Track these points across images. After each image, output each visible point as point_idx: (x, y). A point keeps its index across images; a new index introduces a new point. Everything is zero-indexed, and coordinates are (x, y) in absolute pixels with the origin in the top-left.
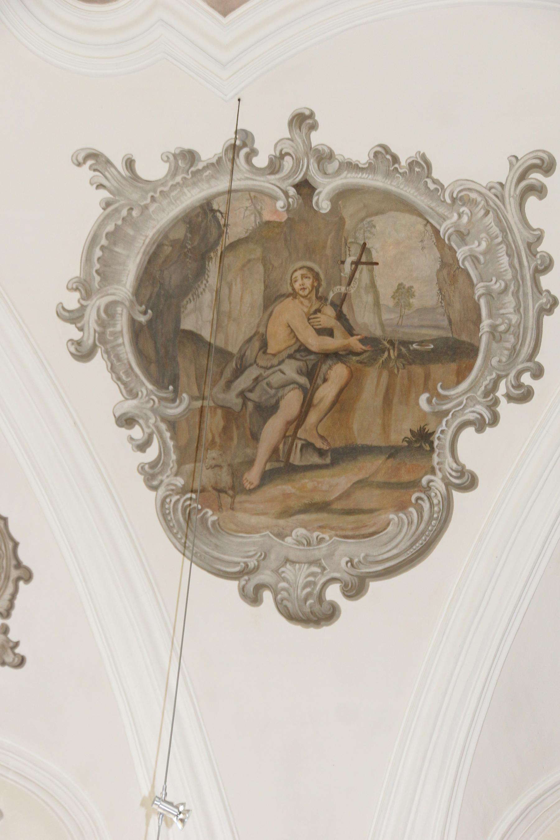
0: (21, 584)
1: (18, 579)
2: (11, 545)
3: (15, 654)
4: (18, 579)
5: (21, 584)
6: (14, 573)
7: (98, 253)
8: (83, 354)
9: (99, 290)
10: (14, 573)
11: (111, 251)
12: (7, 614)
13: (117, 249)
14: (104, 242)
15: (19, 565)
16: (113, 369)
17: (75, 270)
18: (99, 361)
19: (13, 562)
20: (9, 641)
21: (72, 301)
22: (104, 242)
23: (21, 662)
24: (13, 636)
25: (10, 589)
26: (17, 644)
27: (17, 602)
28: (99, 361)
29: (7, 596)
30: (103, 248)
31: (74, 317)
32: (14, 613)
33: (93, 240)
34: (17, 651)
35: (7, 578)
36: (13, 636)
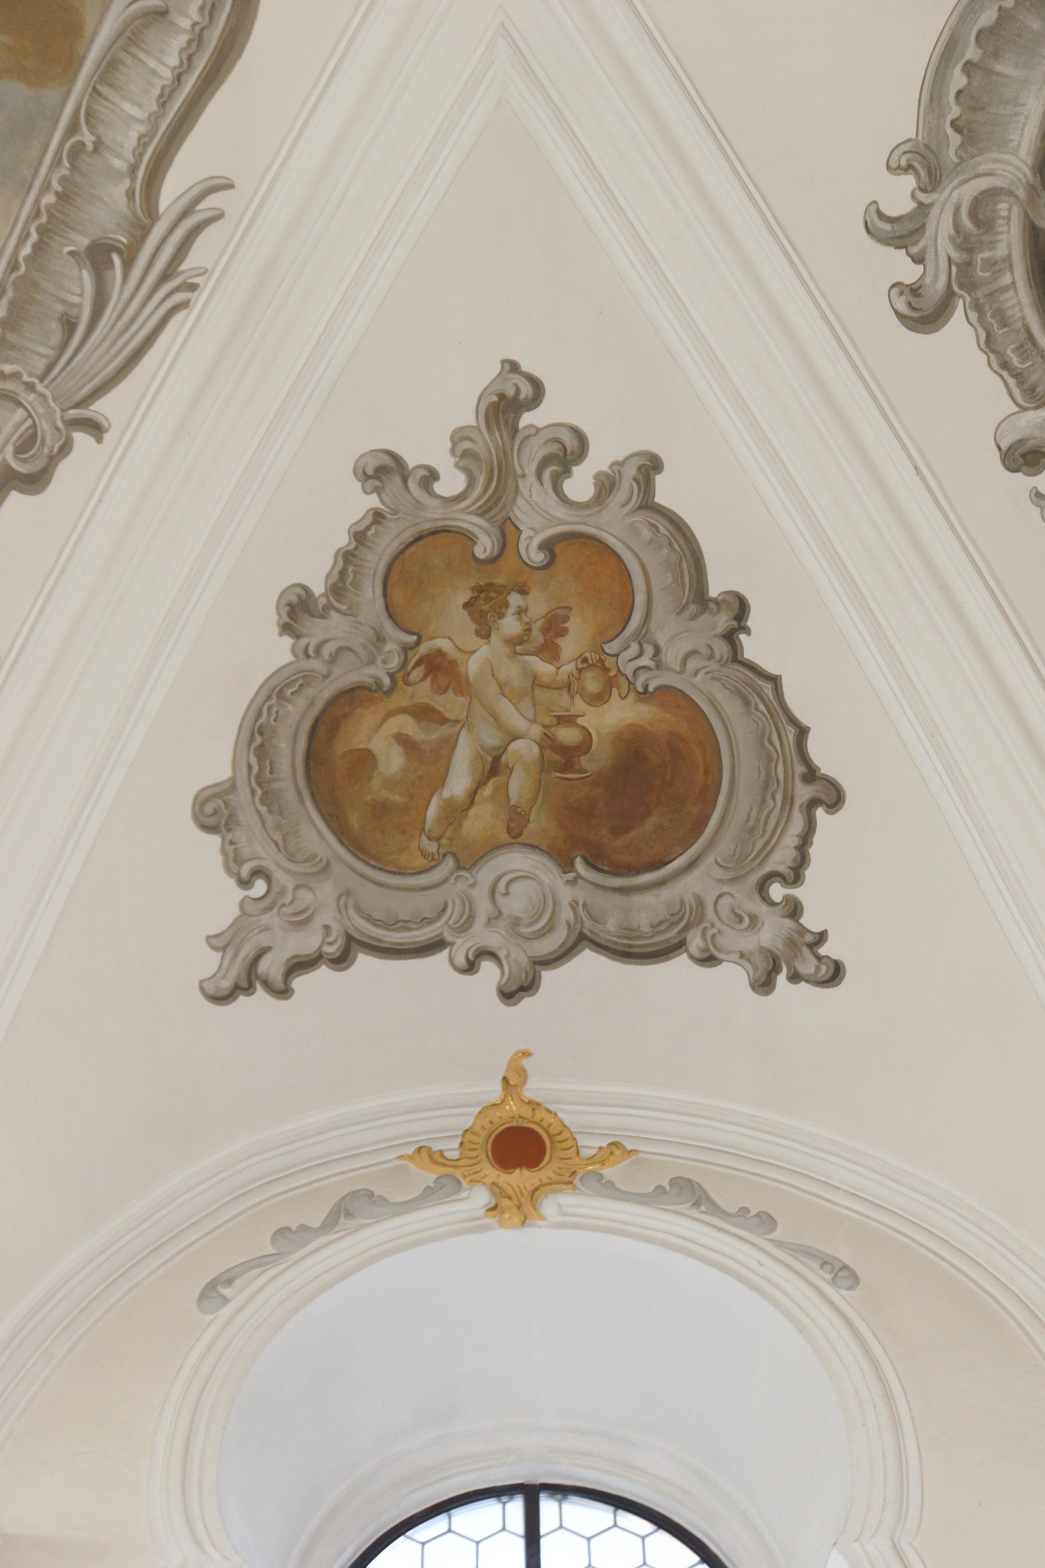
0: (820, 813)
1: (813, 804)
2: (791, 733)
3: (819, 958)
4: (813, 804)
5: (820, 813)
6: (803, 793)
7: (958, 80)
8: (924, 314)
9: (959, 164)
10: (803, 793)
11: (989, 72)
12: (796, 875)
13: (1000, 68)
14: (972, 53)
15: (811, 775)
16: (990, 345)
17: (905, 125)
18: (959, 330)
19: (800, 769)
20: (803, 930)
21: (899, 196)
22: (972, 53)
23: (835, 974)
24: (811, 921)
25: (797, 825)
26: (821, 937)
27: (813, 851)
28: (959, 330)
29: (791, 838)
30: (969, 68)
31: (900, 233)
33: (948, 52)
34: (823, 951)
35: (789, 801)
36: (811, 921)
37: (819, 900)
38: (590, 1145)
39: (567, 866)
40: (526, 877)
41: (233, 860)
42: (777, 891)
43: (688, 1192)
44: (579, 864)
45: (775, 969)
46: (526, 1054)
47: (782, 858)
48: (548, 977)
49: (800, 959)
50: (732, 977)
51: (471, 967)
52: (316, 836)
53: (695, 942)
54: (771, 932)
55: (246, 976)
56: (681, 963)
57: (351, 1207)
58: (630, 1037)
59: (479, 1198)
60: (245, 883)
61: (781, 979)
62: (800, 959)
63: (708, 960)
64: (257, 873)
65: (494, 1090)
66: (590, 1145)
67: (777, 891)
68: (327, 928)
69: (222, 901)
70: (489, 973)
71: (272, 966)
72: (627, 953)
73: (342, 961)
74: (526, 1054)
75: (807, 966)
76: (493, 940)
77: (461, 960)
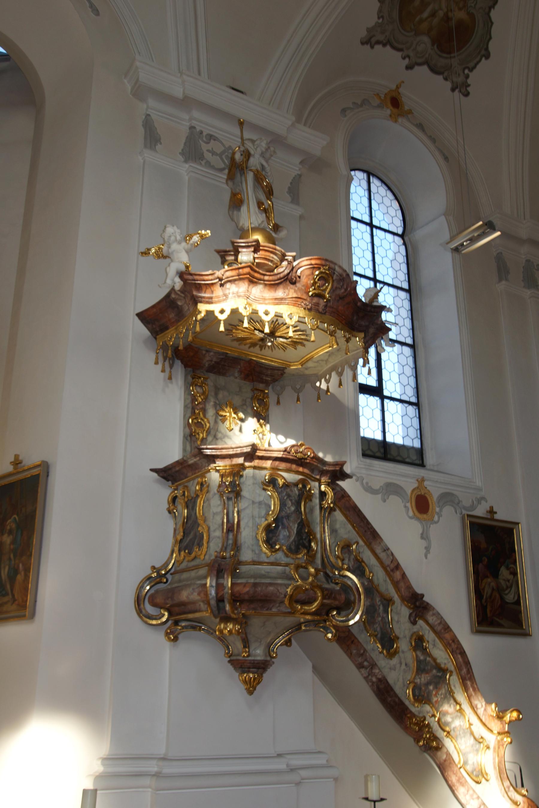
0: (483, 59)
3: (466, 89)
5: (483, 59)
12: (471, 70)
20: (466, 82)
23: (467, 94)
25: (478, 59)
26: (469, 85)
27: (478, 67)
29: (475, 61)
32: (475, 71)
37: (474, 78)
38: (406, 108)
39: (433, 45)
40: (424, 43)
41: (380, 11)
42: (466, 71)
43: (420, 126)
44: (435, 46)
45: (457, 88)
46: (403, 82)
47: (471, 65)
48: (416, 68)
49: (462, 88)
50: (448, 85)
51: (404, 58)
52: (395, 15)
53: (446, 74)
54: (460, 80)
55: (369, 41)
56: (440, 77)
57: (365, 102)
58: (425, 88)
59: (389, 112)
60: (379, 18)
61: (457, 91)
62: (462, 88)
63: (446, 79)
64: (383, 17)
65: (394, 87)
66: (406, 108)
67: (466, 71)
68: (386, 36)
69: (372, 20)
70: (407, 61)
71: (373, 40)
72: (434, 70)
73: (384, 45)
74: (403, 82)
75: (463, 90)
76: (411, 54)
77: (404, 56)
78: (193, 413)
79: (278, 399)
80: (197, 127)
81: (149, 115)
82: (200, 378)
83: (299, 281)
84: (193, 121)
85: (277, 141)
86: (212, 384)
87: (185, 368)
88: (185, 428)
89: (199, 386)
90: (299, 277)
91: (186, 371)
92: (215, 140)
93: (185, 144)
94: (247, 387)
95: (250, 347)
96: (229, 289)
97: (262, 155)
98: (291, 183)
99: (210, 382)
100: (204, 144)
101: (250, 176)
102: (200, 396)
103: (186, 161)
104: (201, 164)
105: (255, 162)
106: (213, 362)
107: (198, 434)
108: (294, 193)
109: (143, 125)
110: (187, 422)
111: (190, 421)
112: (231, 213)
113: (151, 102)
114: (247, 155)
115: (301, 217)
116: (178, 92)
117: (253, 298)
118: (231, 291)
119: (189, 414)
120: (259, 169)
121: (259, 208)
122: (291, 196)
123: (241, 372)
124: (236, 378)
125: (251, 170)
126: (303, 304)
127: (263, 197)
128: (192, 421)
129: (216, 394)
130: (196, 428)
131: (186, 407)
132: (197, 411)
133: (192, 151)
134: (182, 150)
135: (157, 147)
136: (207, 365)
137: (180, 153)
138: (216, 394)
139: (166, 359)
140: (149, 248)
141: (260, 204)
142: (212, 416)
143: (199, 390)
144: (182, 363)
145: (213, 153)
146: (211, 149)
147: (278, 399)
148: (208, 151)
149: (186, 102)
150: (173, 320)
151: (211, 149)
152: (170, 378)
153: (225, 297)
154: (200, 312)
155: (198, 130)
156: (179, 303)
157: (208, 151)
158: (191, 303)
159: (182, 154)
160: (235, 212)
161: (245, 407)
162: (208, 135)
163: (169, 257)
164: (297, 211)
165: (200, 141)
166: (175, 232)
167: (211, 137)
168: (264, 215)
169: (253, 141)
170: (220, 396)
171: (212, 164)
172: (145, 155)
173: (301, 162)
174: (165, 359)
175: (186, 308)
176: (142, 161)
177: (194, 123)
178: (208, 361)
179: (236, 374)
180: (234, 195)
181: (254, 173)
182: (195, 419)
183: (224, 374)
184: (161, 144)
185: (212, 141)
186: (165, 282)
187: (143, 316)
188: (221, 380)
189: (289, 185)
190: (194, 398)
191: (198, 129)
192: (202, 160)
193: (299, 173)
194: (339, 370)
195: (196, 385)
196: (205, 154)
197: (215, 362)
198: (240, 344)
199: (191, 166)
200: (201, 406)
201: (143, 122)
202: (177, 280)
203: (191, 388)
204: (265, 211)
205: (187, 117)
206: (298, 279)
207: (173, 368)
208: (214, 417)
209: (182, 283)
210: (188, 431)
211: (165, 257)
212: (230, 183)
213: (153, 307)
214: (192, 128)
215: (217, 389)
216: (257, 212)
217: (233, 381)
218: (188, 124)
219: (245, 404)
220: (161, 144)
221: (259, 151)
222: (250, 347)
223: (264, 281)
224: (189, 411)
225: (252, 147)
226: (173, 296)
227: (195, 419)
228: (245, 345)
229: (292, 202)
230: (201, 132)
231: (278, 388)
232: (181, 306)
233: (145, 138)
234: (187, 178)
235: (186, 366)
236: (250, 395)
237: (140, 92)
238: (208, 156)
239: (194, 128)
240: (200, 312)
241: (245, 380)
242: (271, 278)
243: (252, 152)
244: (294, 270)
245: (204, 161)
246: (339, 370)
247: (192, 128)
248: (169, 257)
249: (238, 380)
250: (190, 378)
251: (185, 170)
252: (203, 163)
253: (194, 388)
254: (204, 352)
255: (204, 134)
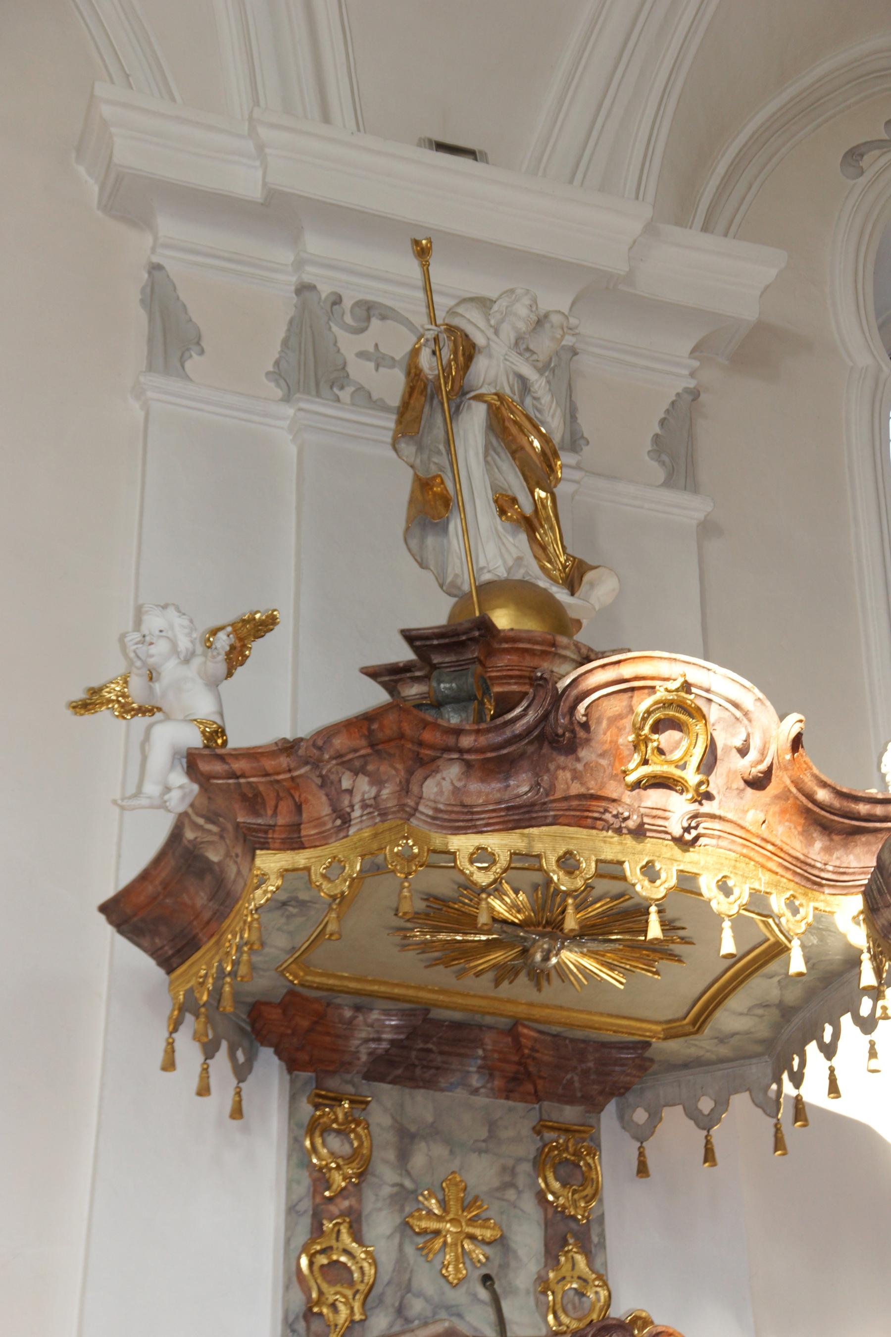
78: (317, 1230)
79: (641, 1154)
80: (319, 287)
81: (158, 267)
82: (339, 1100)
83: (588, 741)
84: (309, 269)
85: (605, 291)
86: (387, 1121)
87: (290, 1070)
88: (287, 1288)
89: (338, 1132)
90: (586, 726)
91: (292, 1082)
92: (383, 318)
93: (285, 343)
94: (518, 1122)
95: (497, 982)
96: (350, 792)
97: (521, 346)
98: (662, 422)
99: (380, 1117)
100: (347, 335)
101: (474, 419)
102: (339, 1167)
103: (287, 399)
104: (338, 400)
105: (491, 371)
106: (384, 1045)
107: (334, 1306)
108: (676, 450)
109: (142, 301)
110: (294, 1268)
111: (304, 1262)
112: (414, 543)
113: (168, 226)
114: (467, 351)
115: (707, 529)
116: (247, 184)
117: (430, 813)
118: (357, 799)
119: (302, 1235)
120: (507, 390)
121: (502, 512)
122: (663, 463)
123: (488, 1070)
124: (475, 1091)
125: (479, 398)
126: (608, 816)
127: (515, 484)
128: (311, 1264)
129: (404, 1156)
130: (325, 1287)
131: (292, 1210)
132: (328, 1225)
133: (310, 365)
134: (277, 363)
135: (188, 365)
136: (364, 1058)
137: (268, 374)
138: (404, 1156)
139: (217, 1049)
140: (95, 684)
141: (504, 504)
142: (390, 1237)
143: (335, 1142)
144: (278, 1053)
145: (380, 360)
146: (371, 349)
147: (641, 1154)
148: (362, 355)
149: (278, 213)
150: (207, 915)
151: (371, 349)
152: (237, 1112)
153: (338, 822)
154: (263, 879)
155: (323, 296)
156: (214, 856)
157: (362, 355)
158: (239, 850)
159: (277, 374)
160: (430, 541)
161: (511, 1194)
162: (358, 304)
163: (159, 709)
164: (689, 509)
165: (335, 328)
166: (172, 627)
167: (368, 311)
168: (523, 537)
169: (484, 303)
170: (418, 1160)
171: (375, 397)
172: (150, 394)
173: (695, 351)
174: (209, 1051)
175: (232, 870)
176: (142, 414)
177: (311, 274)
178: (367, 1041)
179: (475, 1081)
180: (424, 485)
181: (490, 406)
182: (323, 1251)
183: (429, 1084)
184: (202, 352)
185: (375, 322)
186: (139, 793)
187: (123, 913)
188: (421, 1105)
189: (657, 430)
190: (321, 1179)
191: (325, 290)
192: (342, 388)
193: (692, 384)
194: (827, 1038)
195: (326, 1130)
196: (350, 369)
197: (392, 1042)
198: (461, 974)
199: (300, 409)
200: (346, 1204)
201: (143, 291)
202: (179, 778)
203: (308, 1143)
204: (529, 525)
205: (285, 256)
206: (582, 734)
207: (251, 1078)
208: (396, 1240)
209: (196, 787)
210: (298, 1299)
211: (143, 711)
212: (408, 449)
213: (145, 876)
214: (304, 289)
215: (406, 1139)
216: (500, 528)
217: (465, 1103)
218: (294, 279)
219: (512, 1185)
220: (202, 352)
221: (508, 333)
222: (497, 982)
223: (461, 751)
224: (305, 1222)
225: (482, 324)
226: (189, 835)
227: (323, 1251)
228: (478, 975)
229: (669, 483)
230: (337, 300)
231: (640, 1116)
232: (219, 863)
233: (150, 340)
234: (293, 450)
235: (292, 1065)
236: (528, 1148)
237: (131, 199)
238: (361, 372)
239: (312, 288)
240: (263, 879)
241: (507, 1098)
242: (483, 741)
243: (479, 339)
244: (564, 706)
245: (350, 389)
246: (827, 1038)
247: (304, 289)
248: (159, 709)
249: (481, 1100)
250: (306, 1109)
251: (283, 427)
252: (345, 395)
253: (318, 1141)
254: (348, 1013)
255: (347, 303)
